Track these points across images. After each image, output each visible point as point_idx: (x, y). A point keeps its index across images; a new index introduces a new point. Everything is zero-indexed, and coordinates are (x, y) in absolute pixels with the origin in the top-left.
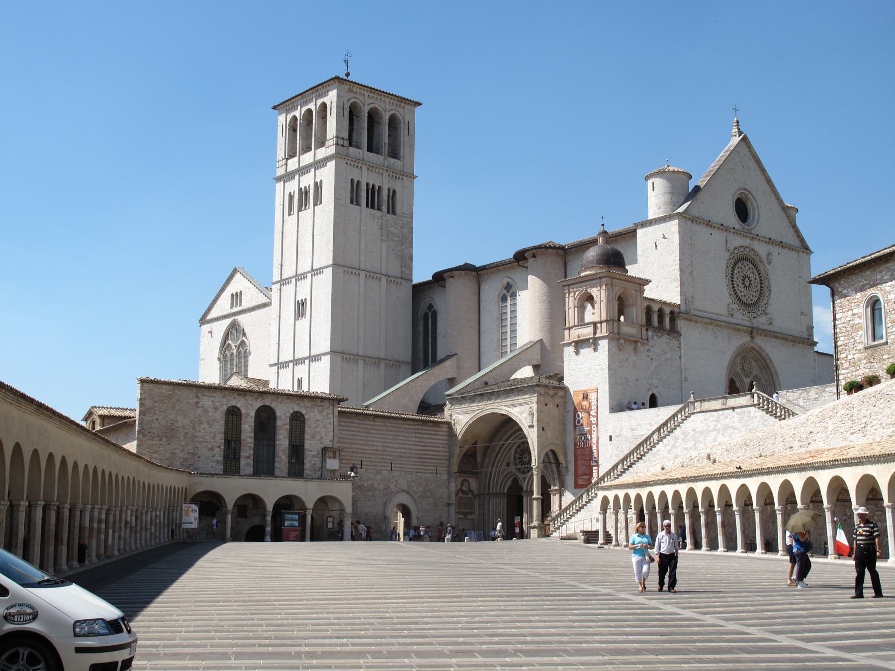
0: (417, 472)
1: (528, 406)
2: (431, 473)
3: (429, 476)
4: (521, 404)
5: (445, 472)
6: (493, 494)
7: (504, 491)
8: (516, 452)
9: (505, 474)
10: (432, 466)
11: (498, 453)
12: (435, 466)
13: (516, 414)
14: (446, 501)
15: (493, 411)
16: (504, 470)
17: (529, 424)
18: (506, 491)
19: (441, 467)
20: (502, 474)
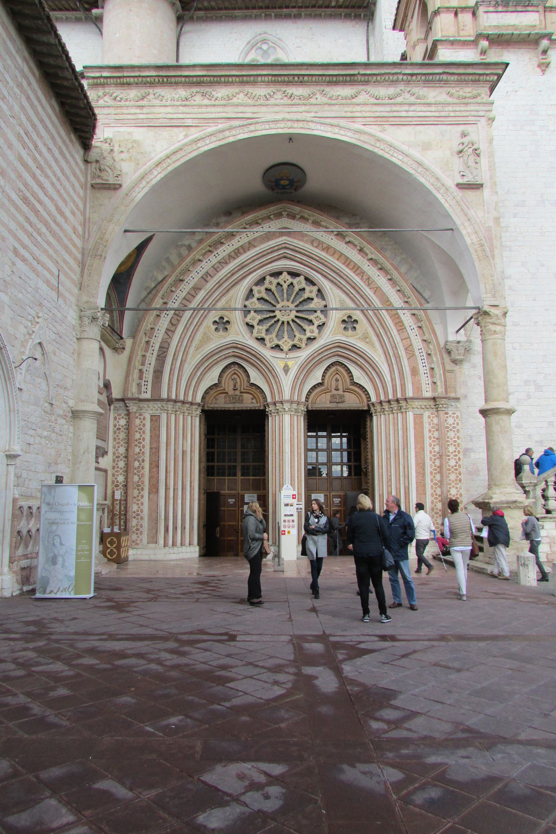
0: (16, 252)
1: (461, 128)
2: (48, 282)
3: (44, 287)
4: (423, 122)
5: (73, 300)
6: (169, 400)
7: (194, 395)
8: (250, 294)
9: (211, 346)
10: (50, 257)
11: (197, 289)
12: (56, 263)
13: (404, 148)
14: (71, 403)
15: (297, 129)
16: (206, 339)
17: (461, 181)
18: (199, 399)
19: (67, 275)
20: (197, 349)
